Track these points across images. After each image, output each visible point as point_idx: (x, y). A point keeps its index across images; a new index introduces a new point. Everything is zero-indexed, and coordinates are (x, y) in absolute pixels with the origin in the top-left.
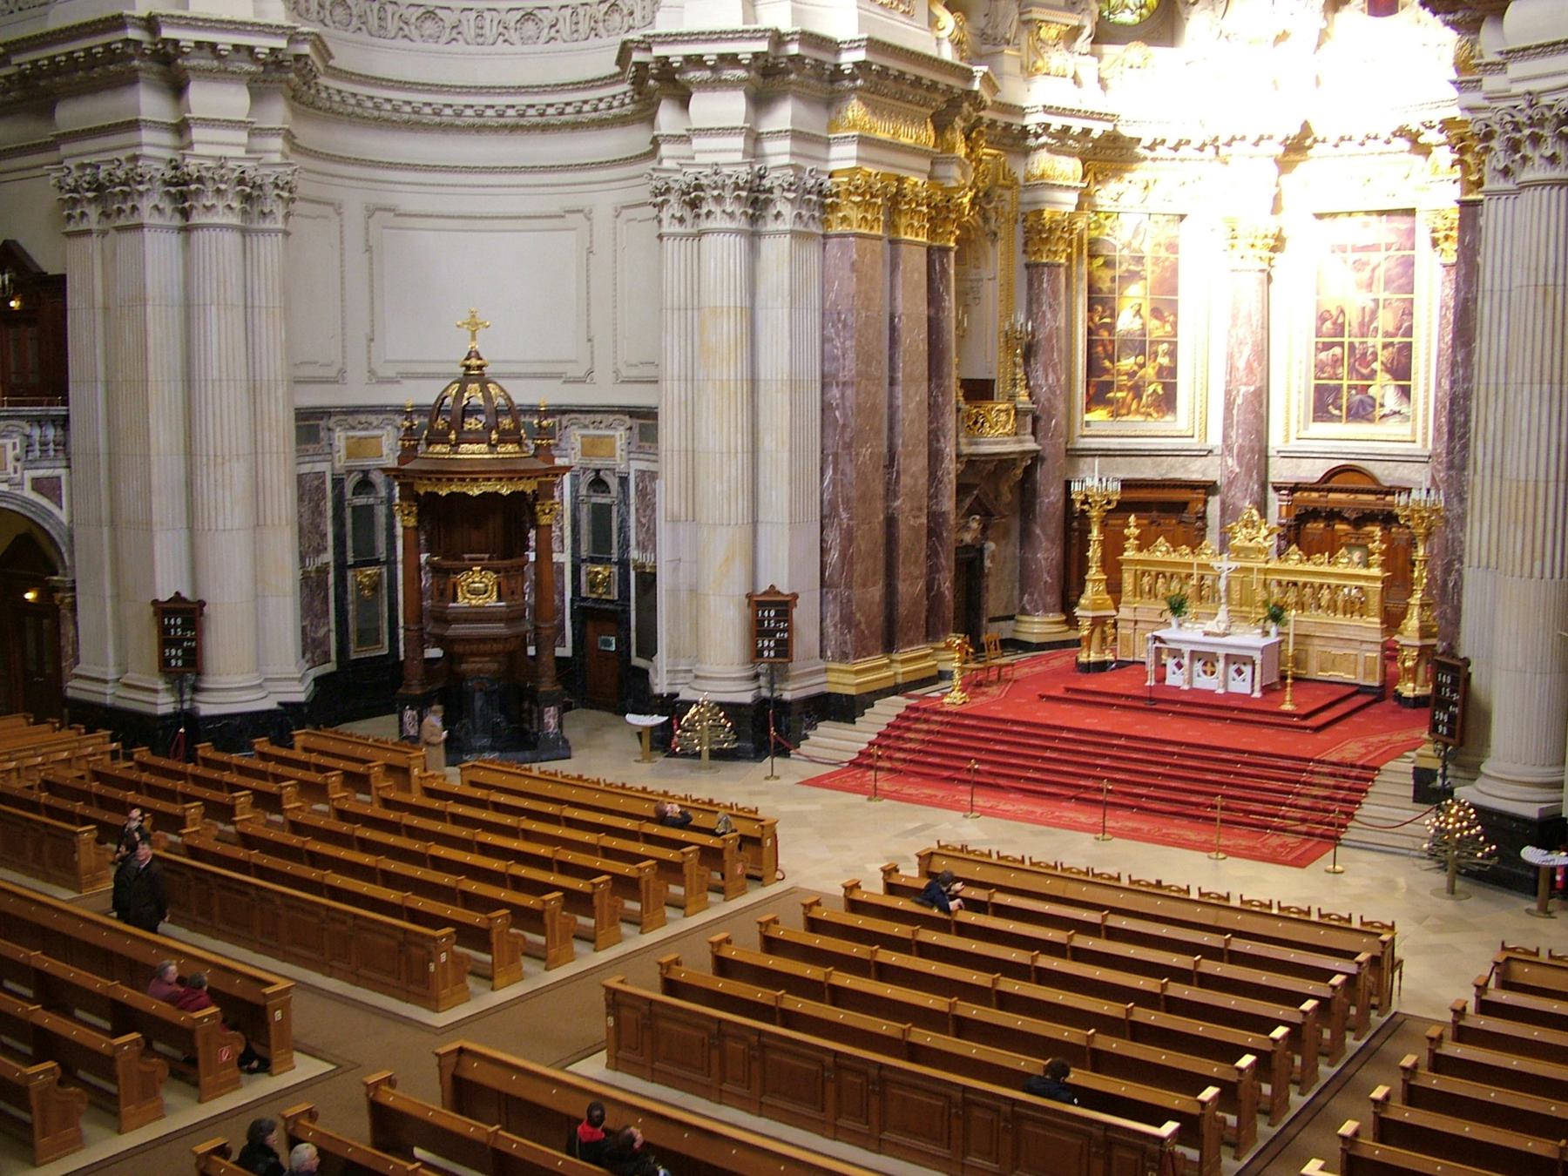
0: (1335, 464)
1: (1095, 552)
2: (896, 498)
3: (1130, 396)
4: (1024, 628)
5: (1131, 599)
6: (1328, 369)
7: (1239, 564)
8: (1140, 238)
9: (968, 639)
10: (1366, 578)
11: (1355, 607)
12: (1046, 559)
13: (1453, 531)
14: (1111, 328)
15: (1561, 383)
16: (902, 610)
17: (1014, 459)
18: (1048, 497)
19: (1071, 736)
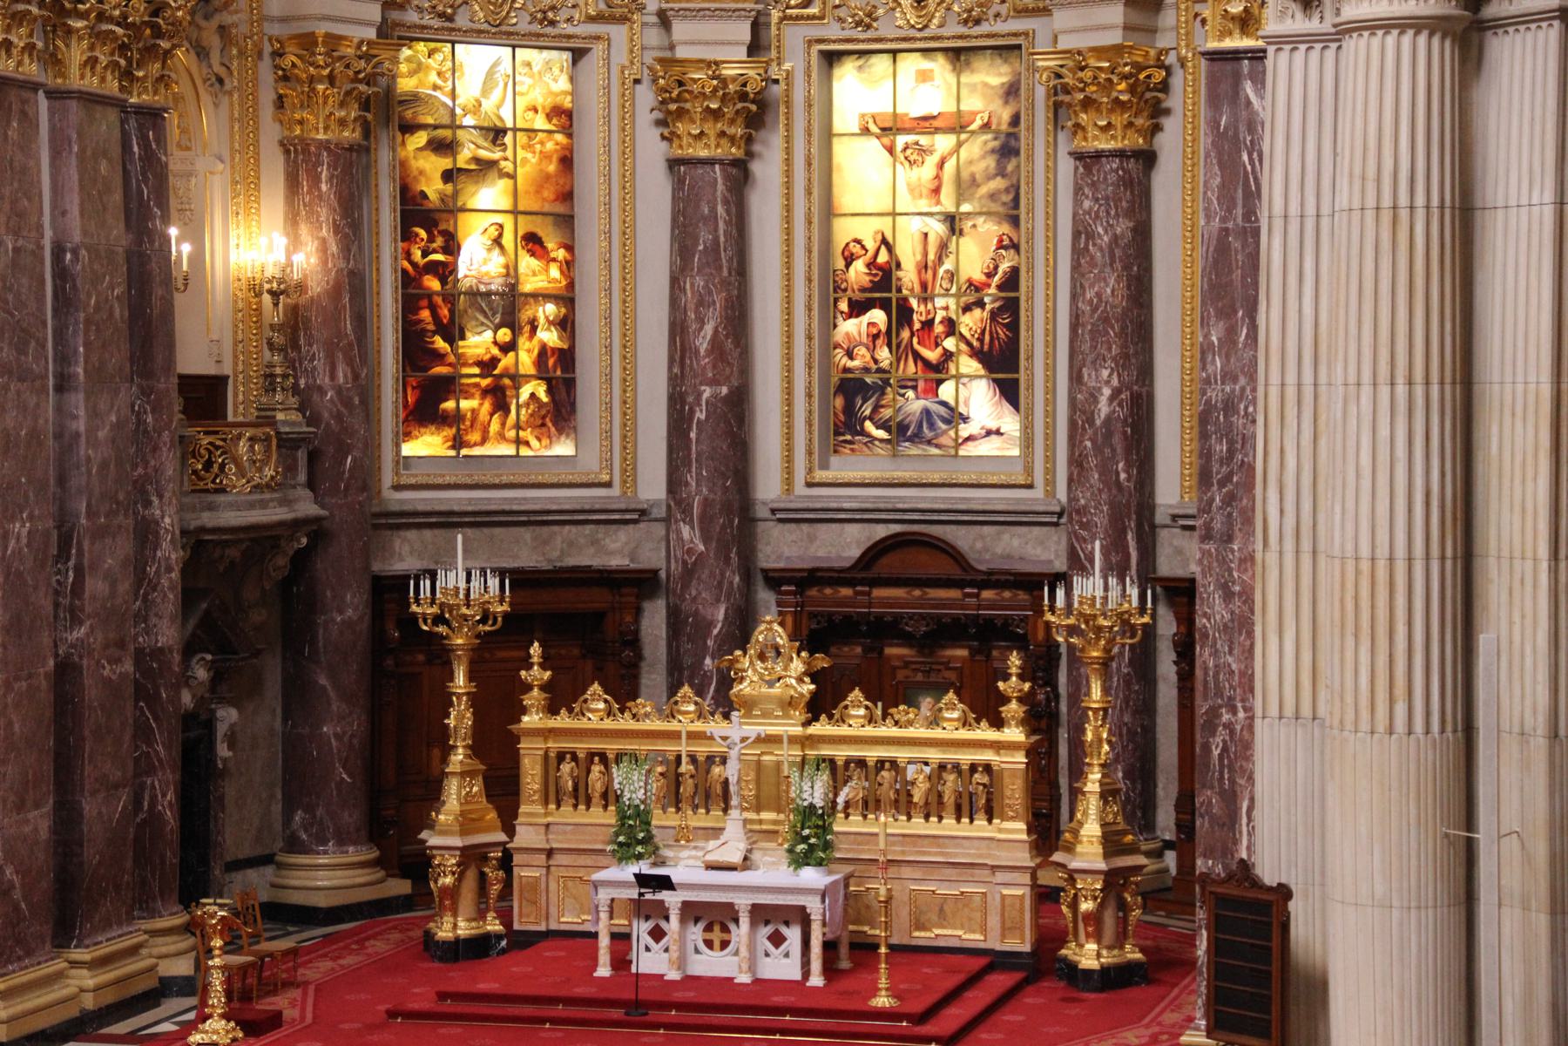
0: (882, 531)
1: (460, 718)
2: (76, 621)
3: (487, 406)
4: (296, 879)
5: (539, 809)
6: (861, 351)
8: (496, 94)
10: (997, 746)
12: (337, 736)
13: (1215, 654)
14: (445, 272)
16: (91, 855)
17: (278, 538)
18: (341, 612)
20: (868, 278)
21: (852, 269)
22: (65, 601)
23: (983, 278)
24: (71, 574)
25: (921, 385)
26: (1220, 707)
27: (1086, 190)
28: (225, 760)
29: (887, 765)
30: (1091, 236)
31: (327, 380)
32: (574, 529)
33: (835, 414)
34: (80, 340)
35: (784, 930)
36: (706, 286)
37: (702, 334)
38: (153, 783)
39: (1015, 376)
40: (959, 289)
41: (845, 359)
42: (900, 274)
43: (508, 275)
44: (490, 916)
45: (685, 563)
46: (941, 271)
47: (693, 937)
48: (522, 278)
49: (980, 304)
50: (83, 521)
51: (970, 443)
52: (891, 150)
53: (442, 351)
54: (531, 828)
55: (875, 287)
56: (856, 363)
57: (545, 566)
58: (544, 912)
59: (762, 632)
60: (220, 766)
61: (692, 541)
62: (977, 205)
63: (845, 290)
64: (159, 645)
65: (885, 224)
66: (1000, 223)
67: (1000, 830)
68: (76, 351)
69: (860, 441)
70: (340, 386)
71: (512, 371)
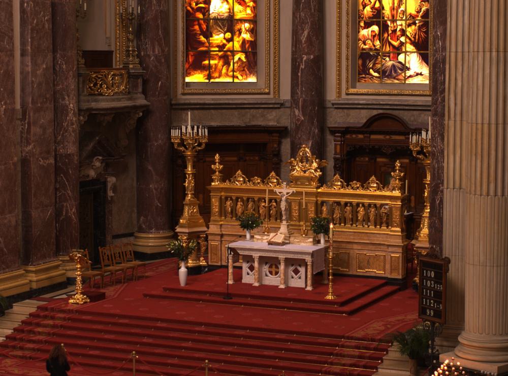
0: (375, 112)
1: (189, 183)
2: (28, 143)
3: (221, 63)
4: (141, 242)
5: (217, 218)
6: (369, 42)
7: (294, 190)
9: (87, 252)
11: (383, 220)
14: (205, 11)
15: (505, 52)
18: (156, 141)
19: (164, 325)
20: (371, 13)
21: (365, 10)
22: (24, 136)
23: (416, 13)
24: (26, 125)
25: (391, 55)
26: (440, 184)
28: (112, 197)
29: (349, 205)
31: (151, 53)
32: (255, 111)
33: (359, 67)
34: (29, 36)
35: (299, 268)
36: (305, 16)
37: (303, 35)
38: (67, 205)
39: (427, 52)
40: (406, 17)
41: (363, 45)
42: (384, 12)
43: (230, 12)
44: (202, 259)
45: (296, 124)
46: (399, 11)
47: (265, 270)
48: (236, 13)
49: (415, 24)
50: (30, 105)
53: (203, 42)
54: (215, 226)
55: (374, 16)
56: (367, 47)
57: (243, 125)
58: (220, 258)
60: (109, 199)
61: (299, 116)
64: (68, 153)
67: (391, 231)
68: (28, 40)
69: (368, 77)
70: (156, 55)
71: (231, 49)
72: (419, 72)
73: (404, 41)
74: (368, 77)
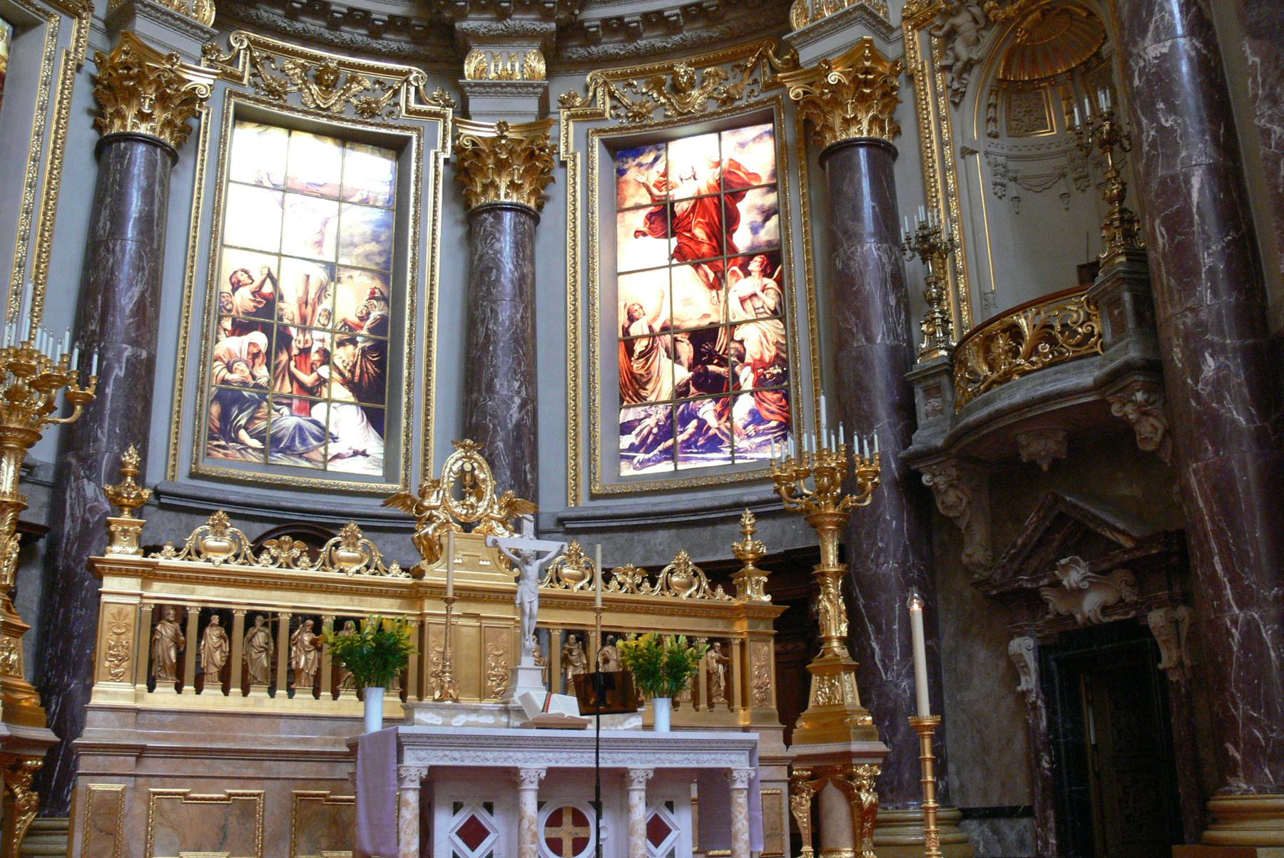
6: (242, 366)
20: (253, 304)
23: (357, 321)
25: (296, 403)
27: (497, 235)
30: (499, 270)
35: (667, 817)
37: (129, 294)
39: (382, 406)
40: (334, 327)
41: (225, 371)
42: (281, 305)
45: (85, 522)
46: (319, 309)
49: (355, 343)
51: (338, 461)
52: (282, 204)
54: (112, 715)
55: (258, 312)
59: (457, 460)
61: (96, 500)
62: (354, 260)
63: (230, 311)
65: (272, 262)
66: (373, 278)
72: (361, 450)
73: (326, 376)
74: (233, 448)
